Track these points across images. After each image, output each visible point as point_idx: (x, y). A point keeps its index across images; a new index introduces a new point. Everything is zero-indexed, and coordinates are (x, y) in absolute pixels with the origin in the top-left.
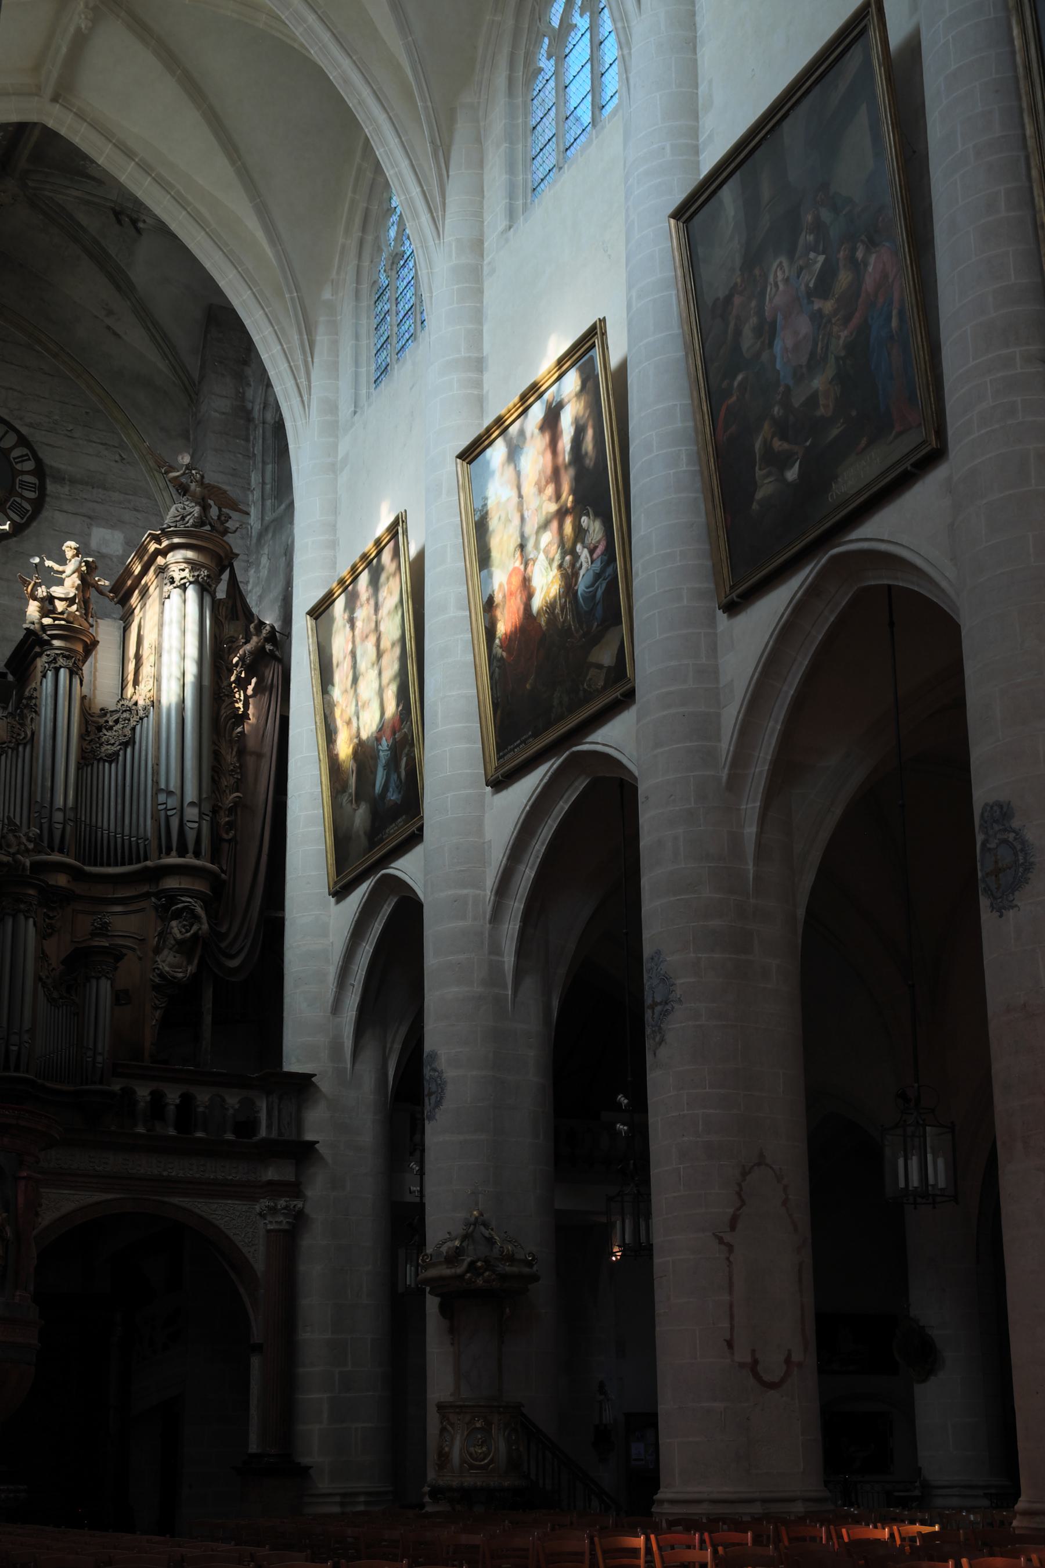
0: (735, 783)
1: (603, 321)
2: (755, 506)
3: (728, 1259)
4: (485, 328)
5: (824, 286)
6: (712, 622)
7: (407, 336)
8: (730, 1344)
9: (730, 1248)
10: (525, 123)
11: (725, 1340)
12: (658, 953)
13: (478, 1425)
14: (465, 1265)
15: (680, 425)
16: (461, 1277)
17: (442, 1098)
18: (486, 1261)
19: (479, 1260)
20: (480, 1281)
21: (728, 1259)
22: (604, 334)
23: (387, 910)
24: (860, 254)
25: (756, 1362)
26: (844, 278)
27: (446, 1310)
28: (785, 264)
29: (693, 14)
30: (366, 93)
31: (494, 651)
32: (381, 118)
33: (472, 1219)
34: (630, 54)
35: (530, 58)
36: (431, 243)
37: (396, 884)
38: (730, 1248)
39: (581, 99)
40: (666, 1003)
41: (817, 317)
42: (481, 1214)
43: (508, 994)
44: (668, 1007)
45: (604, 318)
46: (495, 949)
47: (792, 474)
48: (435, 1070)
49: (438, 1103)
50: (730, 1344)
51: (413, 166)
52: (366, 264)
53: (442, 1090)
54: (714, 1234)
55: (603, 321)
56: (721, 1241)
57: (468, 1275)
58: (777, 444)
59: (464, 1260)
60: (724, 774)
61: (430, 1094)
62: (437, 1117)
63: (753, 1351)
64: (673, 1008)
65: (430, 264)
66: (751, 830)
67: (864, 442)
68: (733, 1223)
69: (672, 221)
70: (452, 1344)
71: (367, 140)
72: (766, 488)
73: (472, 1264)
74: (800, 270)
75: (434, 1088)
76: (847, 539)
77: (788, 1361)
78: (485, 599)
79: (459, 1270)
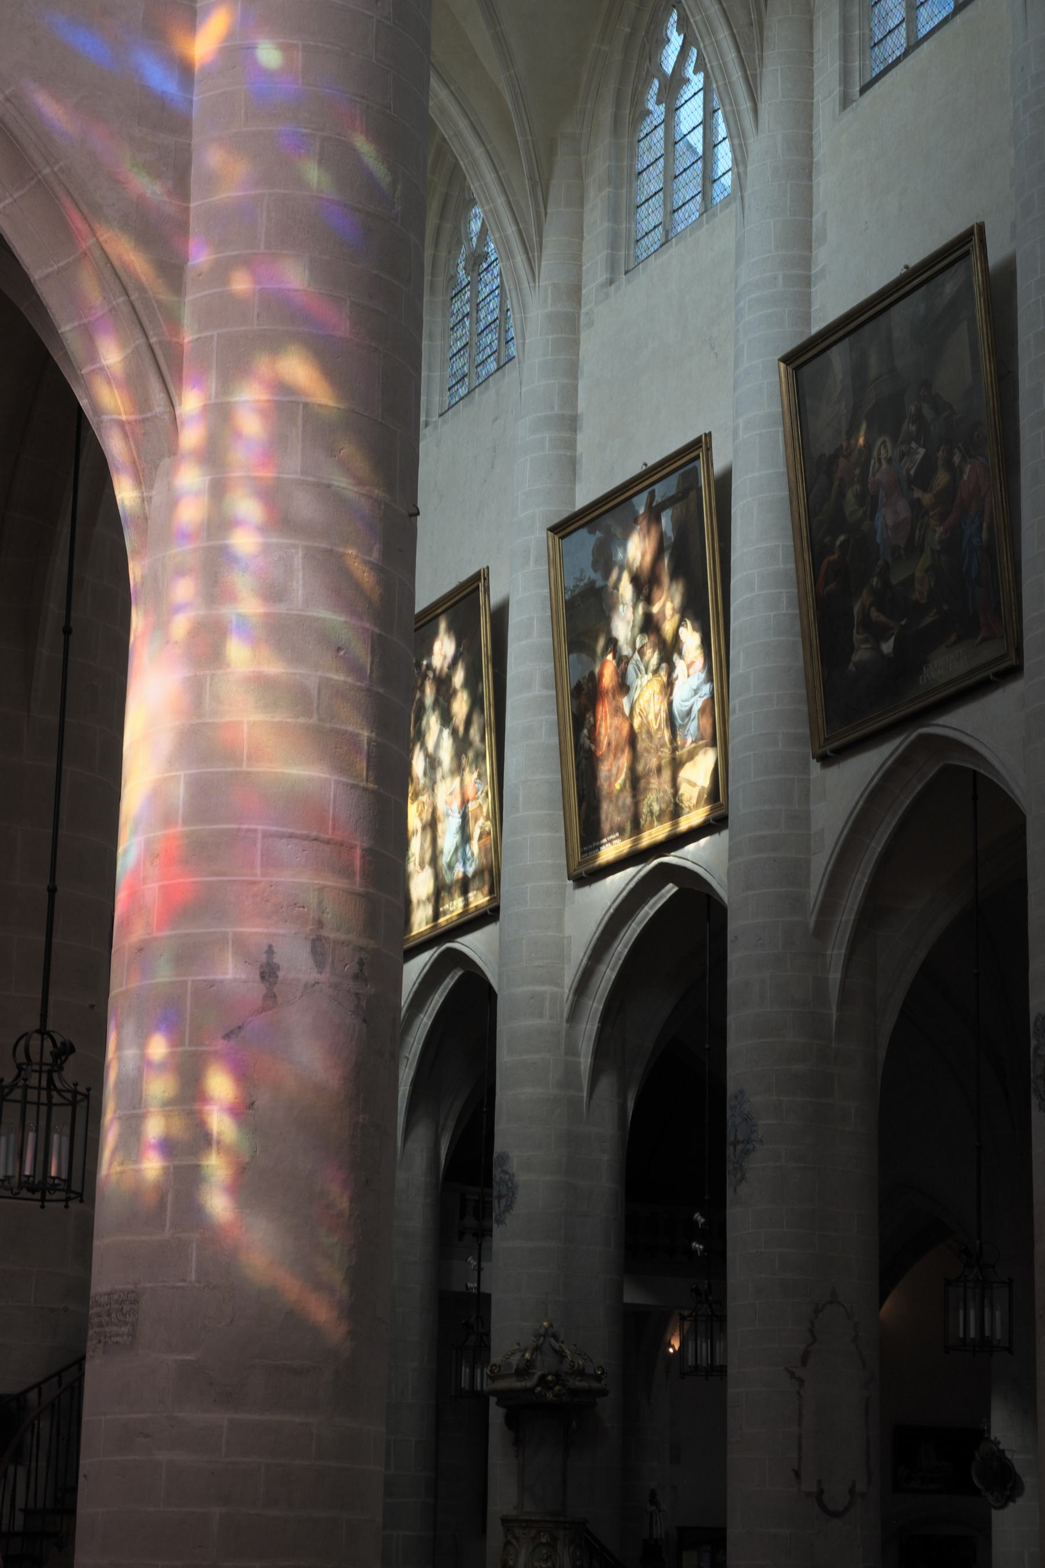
0: (822, 929)
1: (708, 435)
2: (851, 667)
3: (798, 1393)
4: (581, 384)
5: (923, 477)
6: (806, 769)
7: (488, 351)
8: (797, 1474)
9: (801, 1382)
10: (632, 166)
11: (793, 1470)
12: (742, 1092)
13: (544, 1540)
14: (536, 1378)
15: (781, 566)
16: (531, 1390)
17: (512, 1202)
18: (557, 1375)
19: (550, 1374)
20: (550, 1396)
21: (798, 1393)
22: (709, 449)
23: (449, 983)
24: (957, 459)
25: (821, 1492)
26: (942, 478)
27: (512, 1421)
28: (889, 445)
29: (810, 138)
30: (463, 124)
31: (581, 741)
32: (478, 152)
33: (542, 1331)
34: (746, 172)
35: (638, 99)
36: (525, 285)
37: (458, 958)
38: (801, 1382)
39: (693, 94)
40: (748, 1143)
41: (915, 505)
42: (551, 1326)
43: (583, 1097)
44: (750, 1146)
45: (710, 433)
46: (572, 1050)
47: (887, 647)
48: (506, 1173)
49: (509, 1207)
50: (797, 1474)
51: (509, 203)
52: (443, 253)
53: (513, 1194)
54: (786, 1368)
55: (708, 435)
56: (792, 1375)
57: (539, 1389)
58: (875, 614)
59: (534, 1374)
60: (812, 921)
61: (500, 1197)
62: (507, 1221)
63: (819, 1482)
64: (754, 1148)
65: (524, 307)
66: (835, 976)
67: (953, 638)
68: (804, 1360)
69: (782, 365)
70: (517, 1457)
71: (456, 164)
72: (861, 654)
73: (543, 1378)
74: (903, 455)
75: (504, 1192)
76: (935, 722)
77: (852, 1491)
78: (574, 684)
79: (529, 1384)
